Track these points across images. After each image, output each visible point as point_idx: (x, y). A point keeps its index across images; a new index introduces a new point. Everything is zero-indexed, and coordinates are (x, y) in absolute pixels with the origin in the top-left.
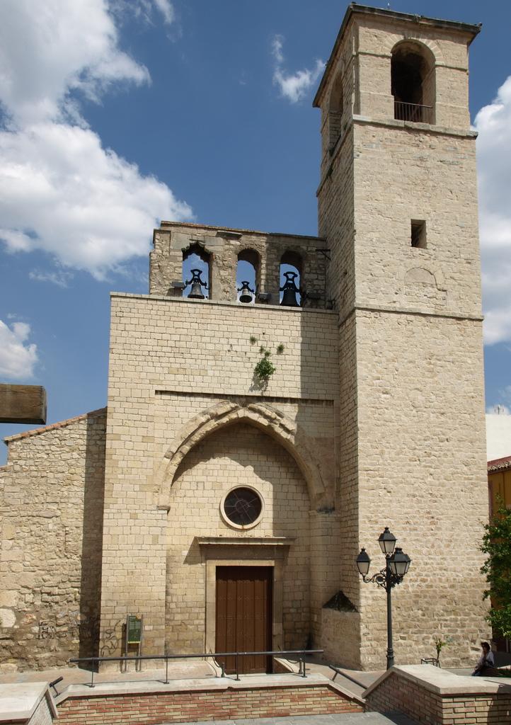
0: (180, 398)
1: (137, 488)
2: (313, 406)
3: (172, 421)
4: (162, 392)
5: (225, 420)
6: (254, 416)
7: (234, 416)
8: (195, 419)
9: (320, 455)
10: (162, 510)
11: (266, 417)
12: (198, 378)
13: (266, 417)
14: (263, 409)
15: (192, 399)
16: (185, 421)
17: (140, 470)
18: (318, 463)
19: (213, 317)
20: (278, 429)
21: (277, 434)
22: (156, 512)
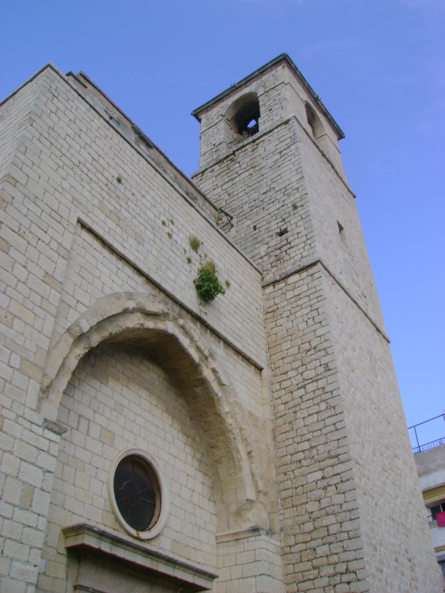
0: (106, 252)
1: (16, 361)
2: (244, 364)
3: (90, 278)
4: (84, 226)
5: (150, 324)
6: (185, 342)
7: (161, 325)
8: (117, 296)
9: (253, 438)
10: (51, 430)
11: (198, 349)
12: (132, 241)
13: (198, 349)
14: (196, 337)
15: (120, 264)
16: (108, 291)
17: (28, 327)
18: (250, 449)
19: (157, 186)
20: (207, 373)
21: (203, 382)
22: (39, 430)
